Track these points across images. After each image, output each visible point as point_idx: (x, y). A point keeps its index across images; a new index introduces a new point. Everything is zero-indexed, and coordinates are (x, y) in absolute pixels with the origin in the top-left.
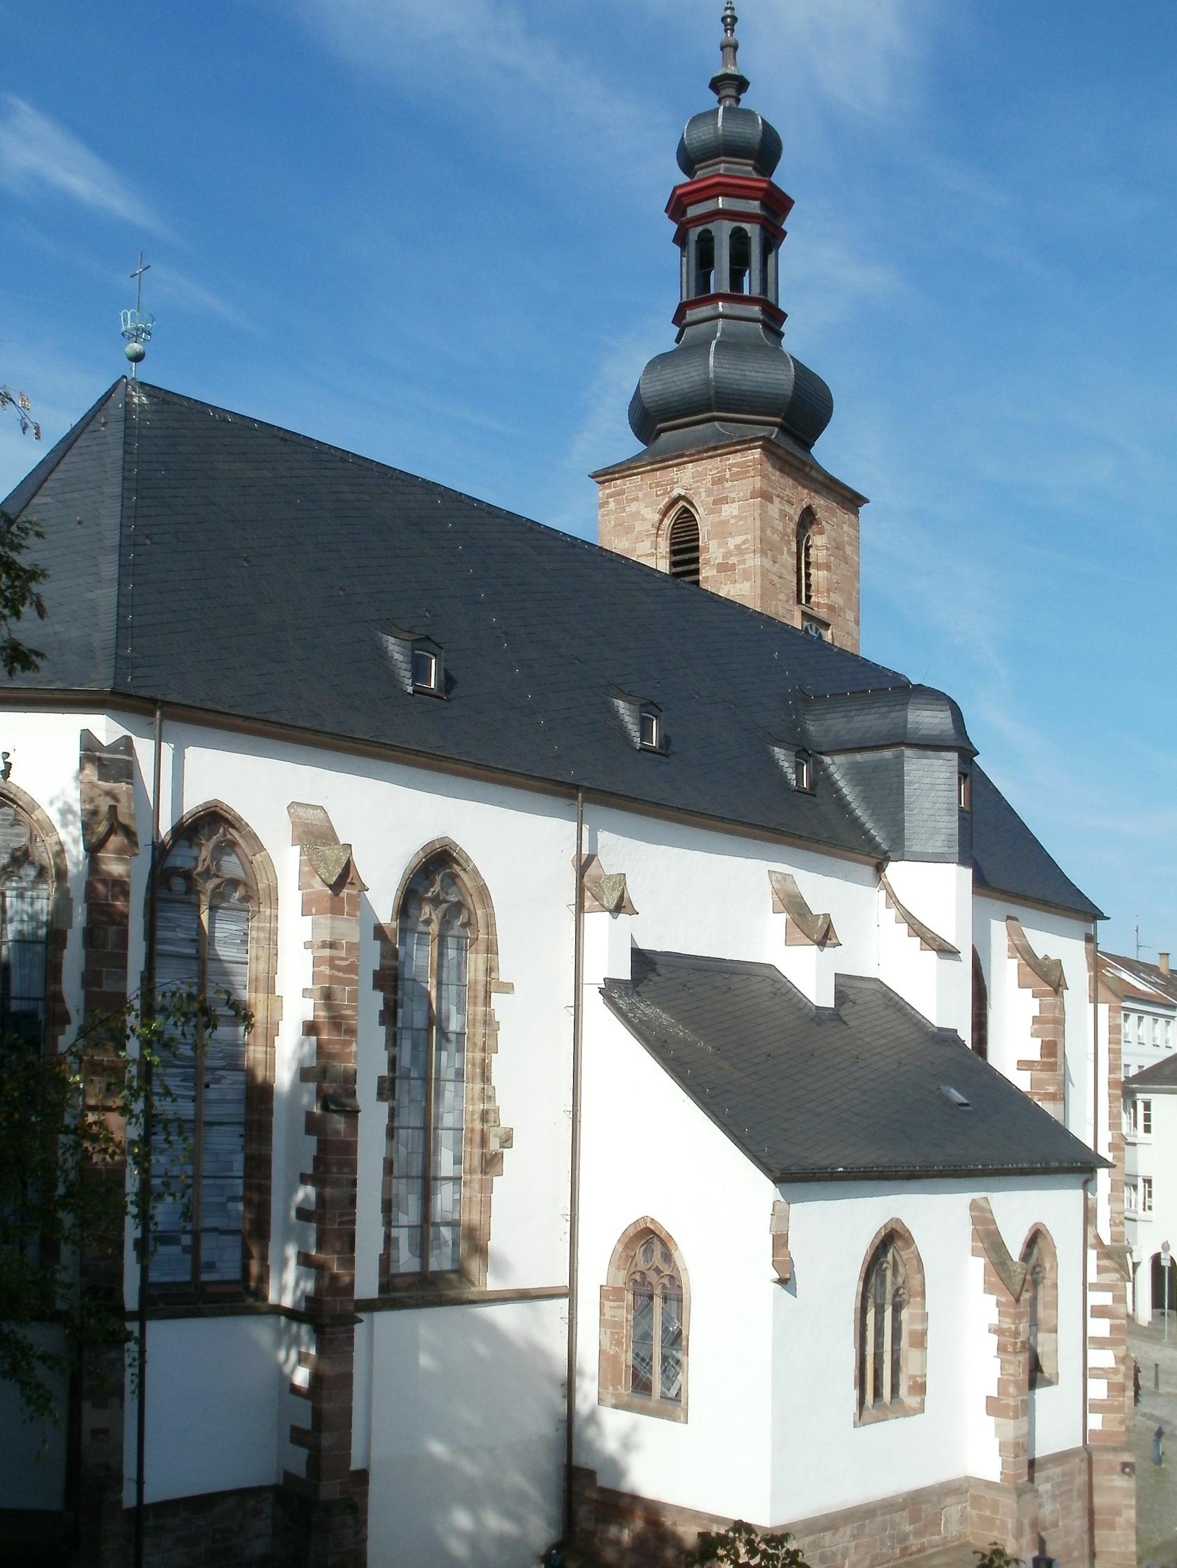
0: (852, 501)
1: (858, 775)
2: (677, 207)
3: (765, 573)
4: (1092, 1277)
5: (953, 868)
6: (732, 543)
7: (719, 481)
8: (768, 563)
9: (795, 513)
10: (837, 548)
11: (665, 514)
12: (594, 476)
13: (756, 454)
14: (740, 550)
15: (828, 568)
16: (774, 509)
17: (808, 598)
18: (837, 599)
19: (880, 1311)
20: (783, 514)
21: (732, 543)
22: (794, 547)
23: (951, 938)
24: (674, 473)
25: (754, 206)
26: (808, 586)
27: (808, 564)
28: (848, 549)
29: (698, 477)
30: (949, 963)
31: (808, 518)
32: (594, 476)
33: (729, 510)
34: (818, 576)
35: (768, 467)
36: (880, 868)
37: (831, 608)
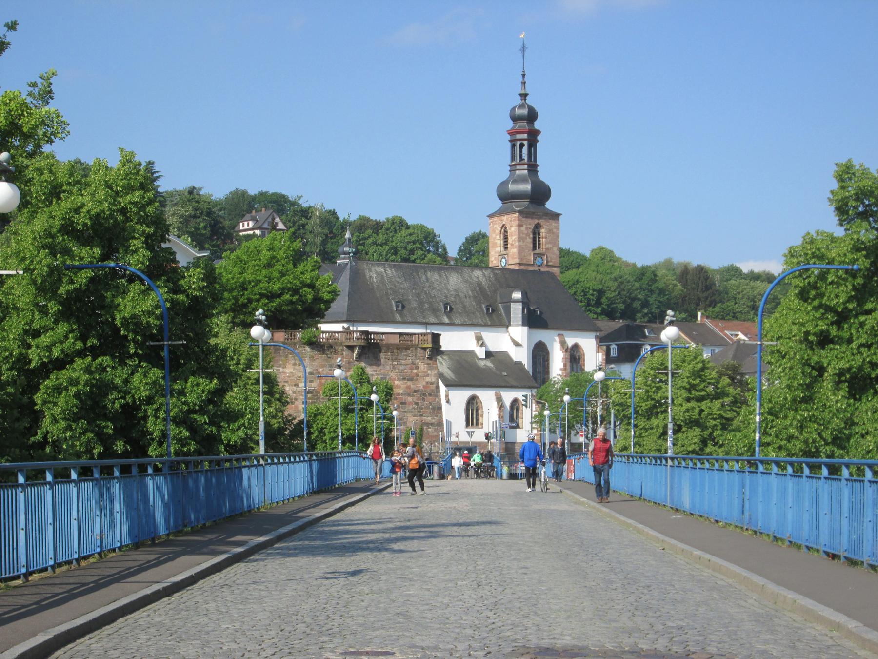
0: (556, 216)
1: (504, 308)
2: (512, 133)
3: (519, 246)
4: (534, 409)
5: (521, 327)
6: (514, 238)
7: (511, 221)
8: (521, 243)
9: (532, 226)
10: (550, 231)
11: (502, 228)
12: (488, 216)
13: (517, 214)
14: (514, 240)
15: (546, 238)
16: (523, 228)
17: (539, 248)
18: (549, 246)
19: (472, 410)
20: (527, 229)
21: (514, 238)
22: (531, 236)
23: (520, 342)
24: (503, 218)
25: (525, 136)
26: (539, 244)
27: (539, 238)
28: (555, 230)
29: (507, 219)
30: (519, 348)
31: (538, 226)
32: (488, 216)
33: (513, 229)
34: (543, 241)
35: (521, 217)
36: (507, 328)
37: (547, 249)
